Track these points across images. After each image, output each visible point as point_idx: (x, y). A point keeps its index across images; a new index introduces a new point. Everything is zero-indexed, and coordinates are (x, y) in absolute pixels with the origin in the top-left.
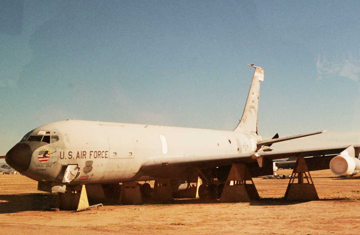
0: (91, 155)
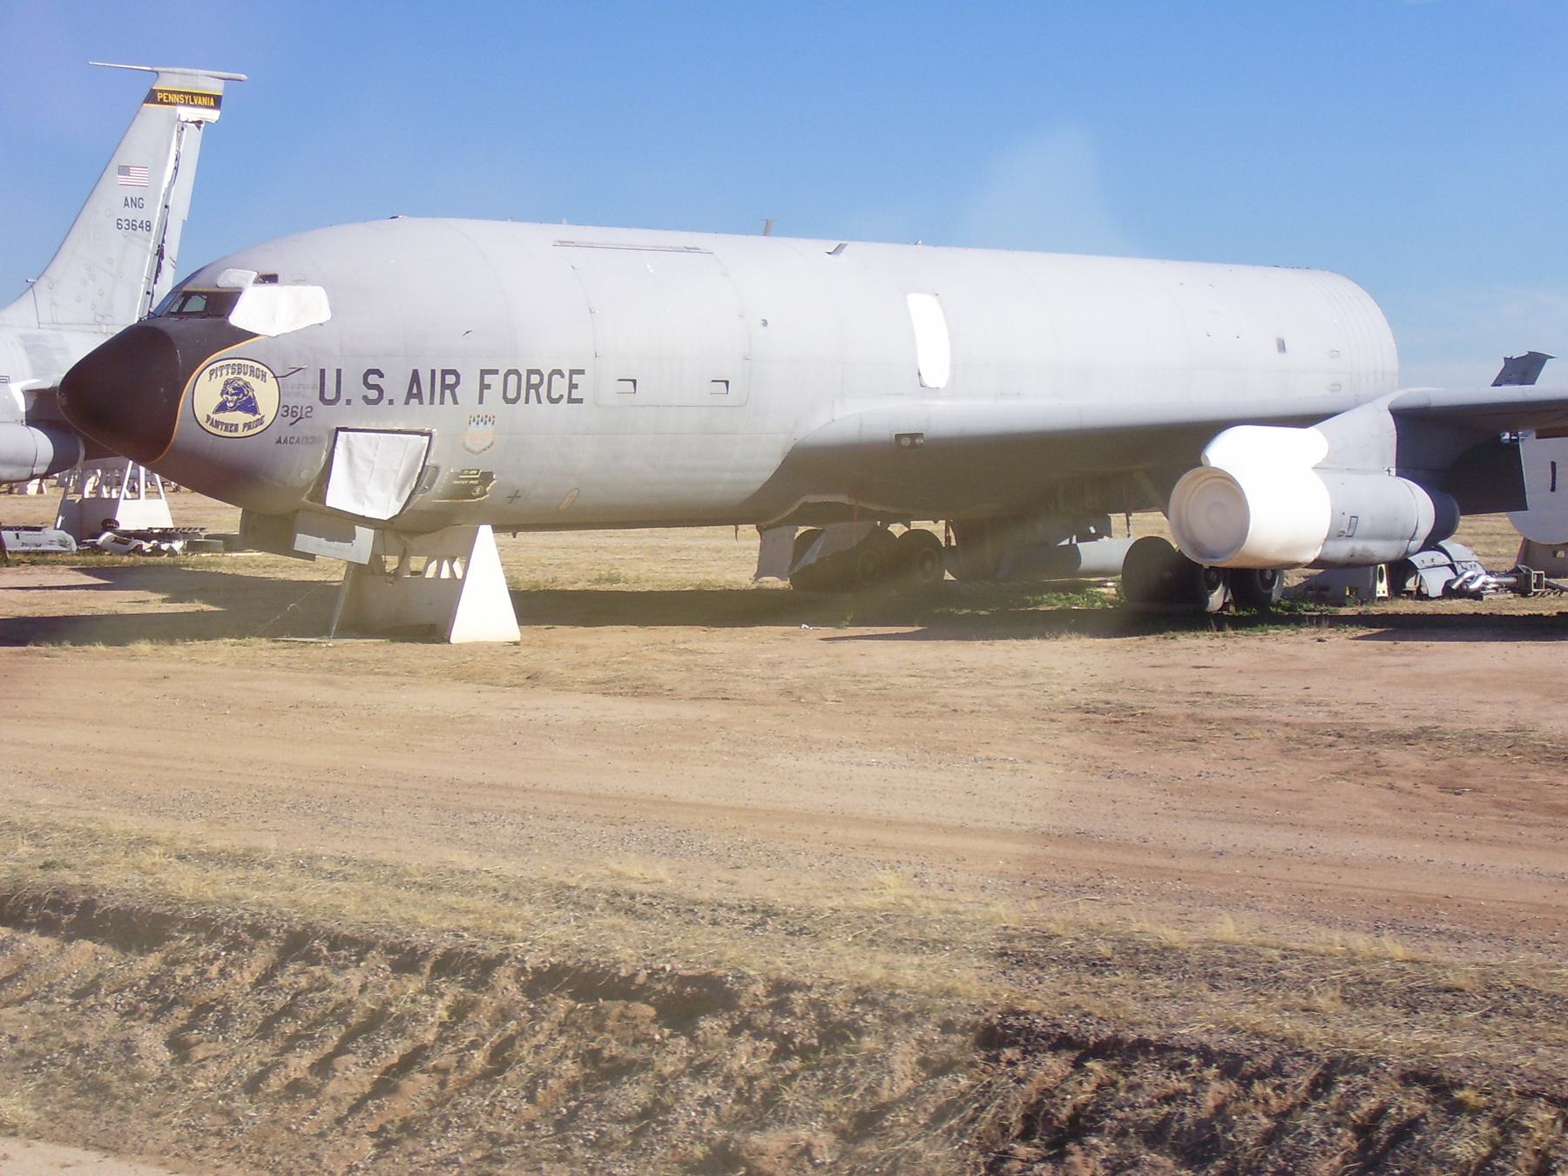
0: (488, 387)
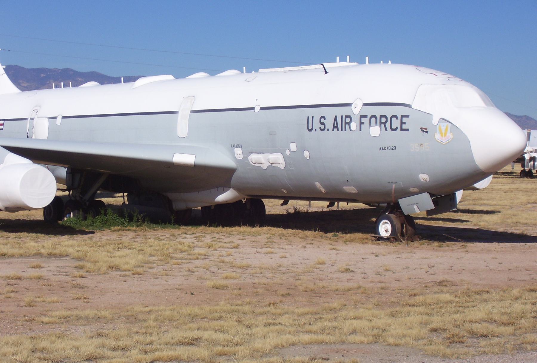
0: (363, 123)
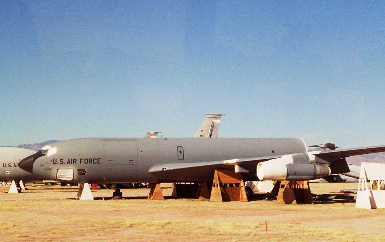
0: (82, 161)
